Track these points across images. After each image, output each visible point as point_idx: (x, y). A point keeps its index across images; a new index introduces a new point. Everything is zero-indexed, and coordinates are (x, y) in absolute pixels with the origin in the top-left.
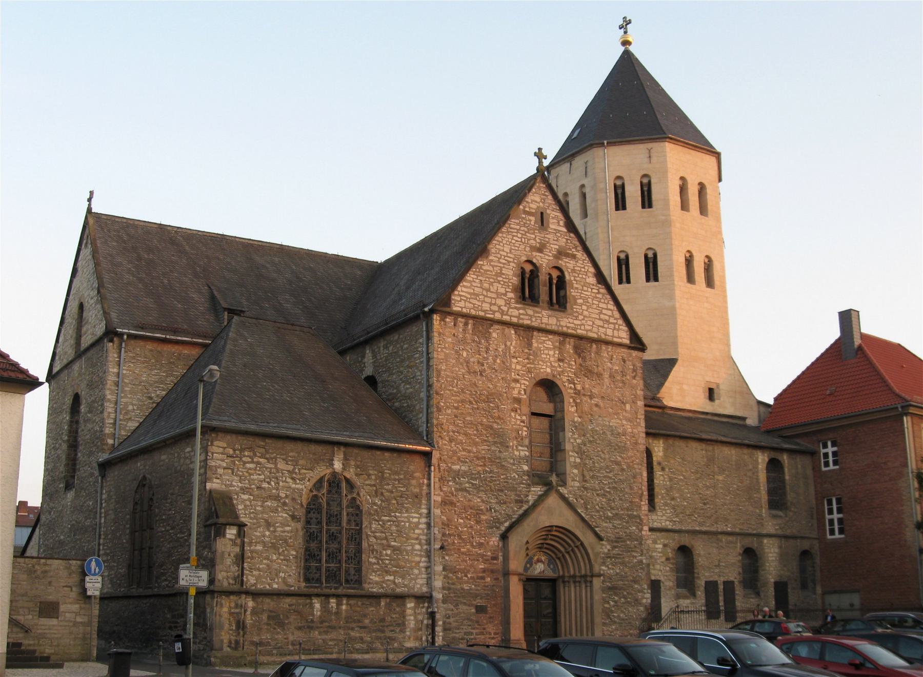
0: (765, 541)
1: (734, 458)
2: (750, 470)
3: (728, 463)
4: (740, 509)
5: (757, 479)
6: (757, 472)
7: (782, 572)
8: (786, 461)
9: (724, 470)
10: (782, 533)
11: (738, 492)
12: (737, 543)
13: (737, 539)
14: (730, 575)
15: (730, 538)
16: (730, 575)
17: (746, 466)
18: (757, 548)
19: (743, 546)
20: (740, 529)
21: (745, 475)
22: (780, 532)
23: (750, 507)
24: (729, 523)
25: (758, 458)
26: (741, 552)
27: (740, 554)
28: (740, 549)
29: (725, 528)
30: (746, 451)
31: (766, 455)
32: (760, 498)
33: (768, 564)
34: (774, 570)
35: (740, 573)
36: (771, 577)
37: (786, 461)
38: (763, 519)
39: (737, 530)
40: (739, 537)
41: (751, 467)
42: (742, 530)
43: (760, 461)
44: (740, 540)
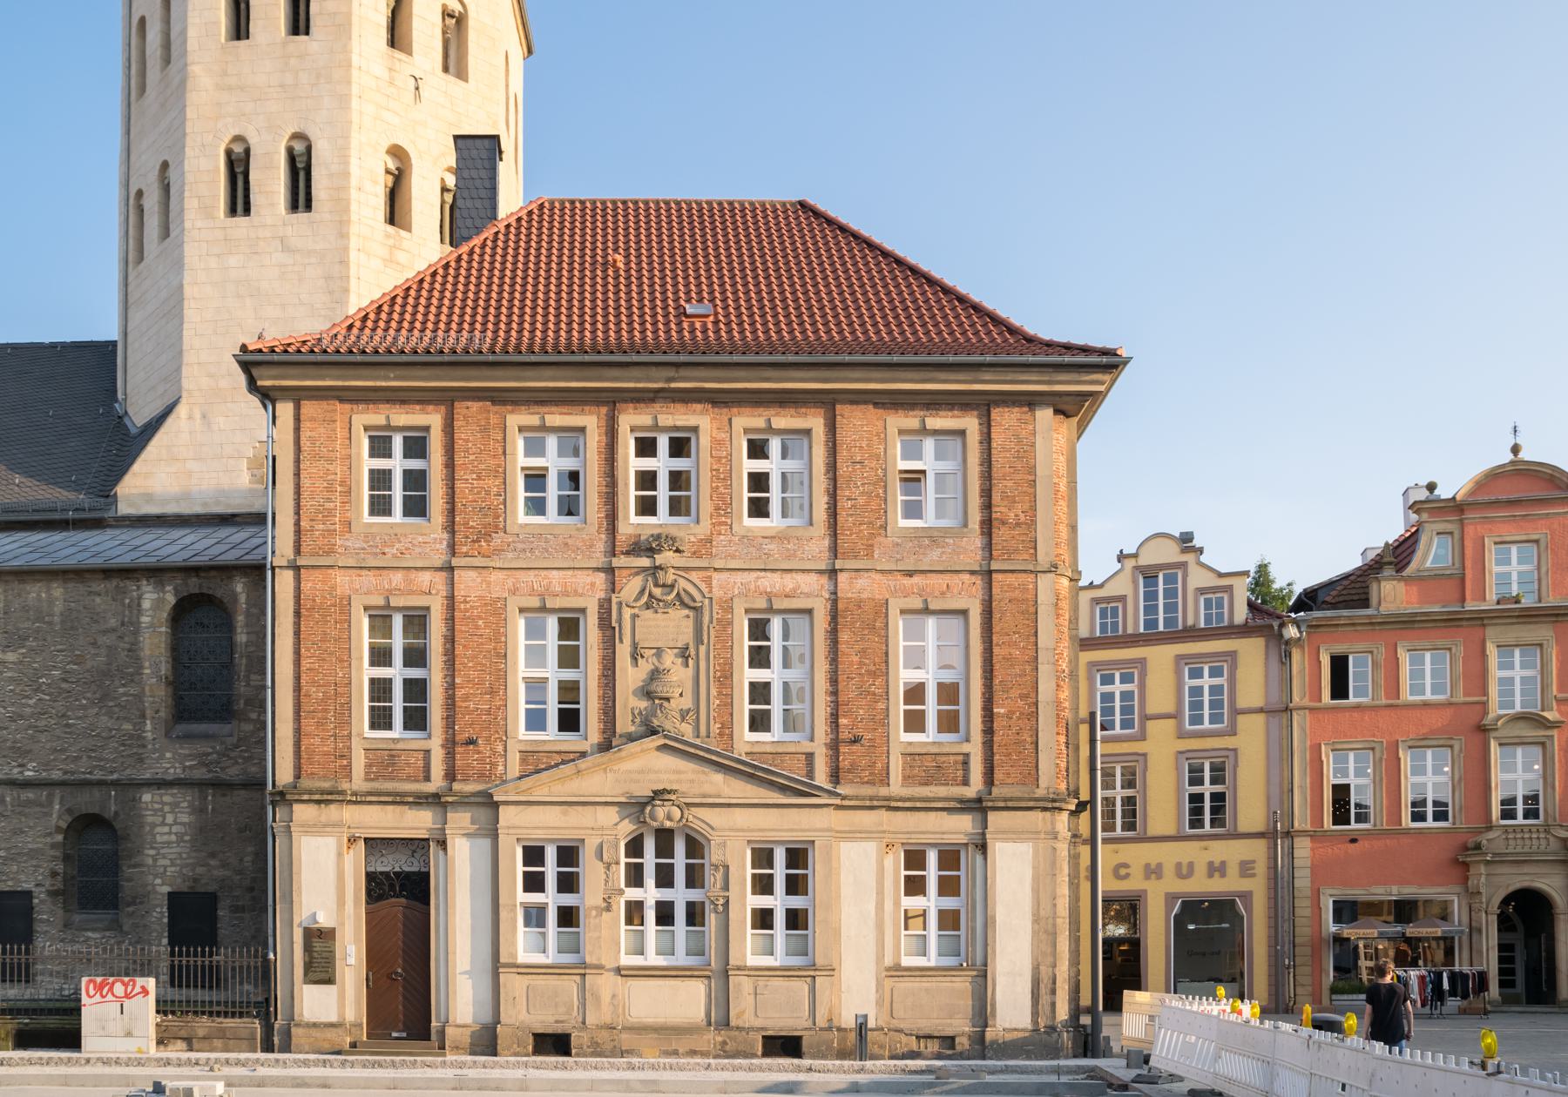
0: (147, 797)
1: (59, 607)
2: (114, 630)
3: (38, 619)
4: (68, 725)
5: (133, 650)
6: (136, 633)
7: (199, 870)
8: (243, 598)
9: (26, 639)
10: (211, 775)
11: (64, 685)
12: (50, 803)
13: (50, 797)
14: (23, 877)
15: (30, 794)
16: (23, 877)
17: (96, 622)
18: (116, 813)
19: (69, 811)
20: (66, 773)
21: (94, 644)
22: (200, 774)
23: (104, 718)
24: (31, 760)
25: (140, 598)
26: (64, 825)
27: (58, 829)
28: (60, 817)
29: (16, 771)
30: (99, 586)
31: (168, 588)
32: (139, 697)
33: (152, 852)
34: (173, 865)
35: (54, 874)
36: (158, 881)
37: (243, 598)
38: (144, 746)
39: (56, 775)
40: (58, 792)
41: (113, 622)
42: (73, 773)
43: (146, 604)
44: (62, 798)
